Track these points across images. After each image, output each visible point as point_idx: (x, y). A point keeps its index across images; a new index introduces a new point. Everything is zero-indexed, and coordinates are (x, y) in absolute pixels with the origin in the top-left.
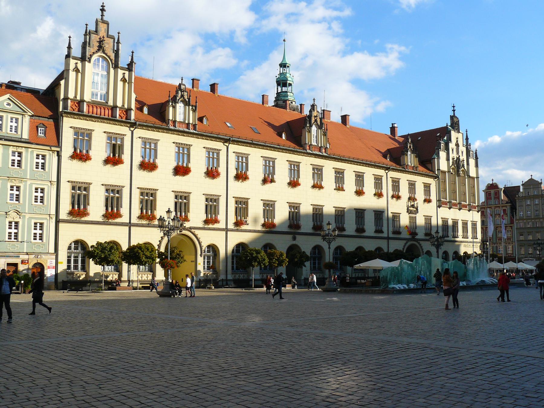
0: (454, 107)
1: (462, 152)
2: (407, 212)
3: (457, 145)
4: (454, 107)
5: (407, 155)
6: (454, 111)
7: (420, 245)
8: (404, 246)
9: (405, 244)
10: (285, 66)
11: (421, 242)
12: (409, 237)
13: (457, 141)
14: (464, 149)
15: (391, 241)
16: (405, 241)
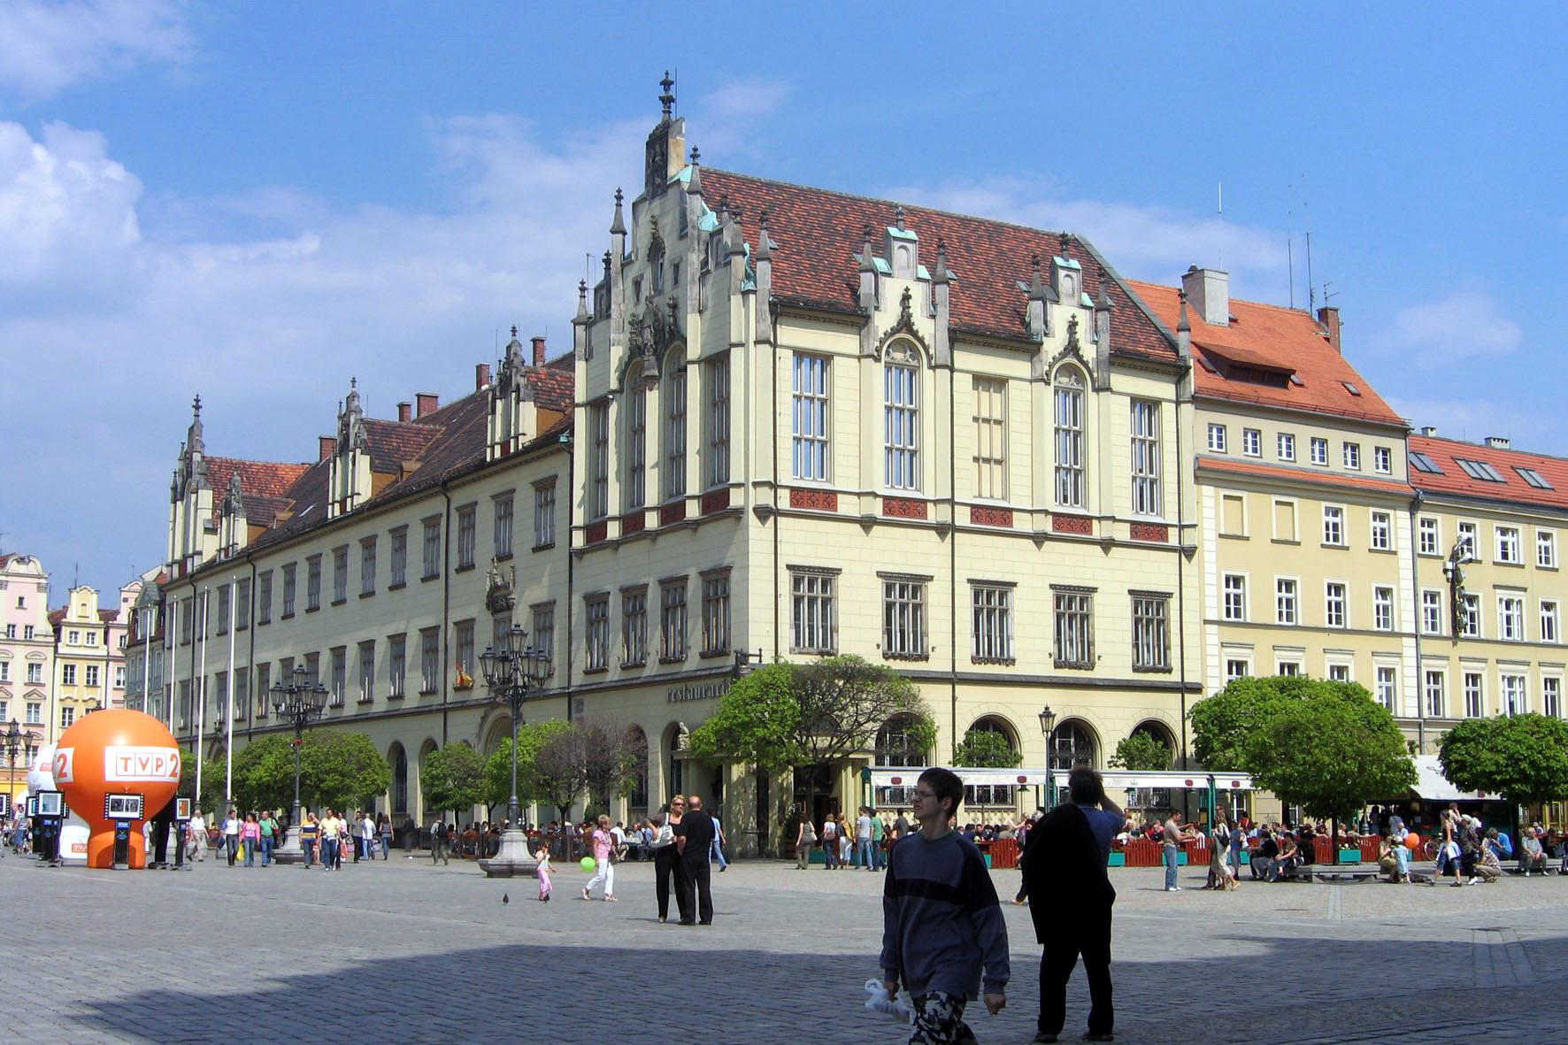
0: (667, 84)
4: (667, 84)
6: (667, 101)
15: (455, 719)
16: (480, 712)
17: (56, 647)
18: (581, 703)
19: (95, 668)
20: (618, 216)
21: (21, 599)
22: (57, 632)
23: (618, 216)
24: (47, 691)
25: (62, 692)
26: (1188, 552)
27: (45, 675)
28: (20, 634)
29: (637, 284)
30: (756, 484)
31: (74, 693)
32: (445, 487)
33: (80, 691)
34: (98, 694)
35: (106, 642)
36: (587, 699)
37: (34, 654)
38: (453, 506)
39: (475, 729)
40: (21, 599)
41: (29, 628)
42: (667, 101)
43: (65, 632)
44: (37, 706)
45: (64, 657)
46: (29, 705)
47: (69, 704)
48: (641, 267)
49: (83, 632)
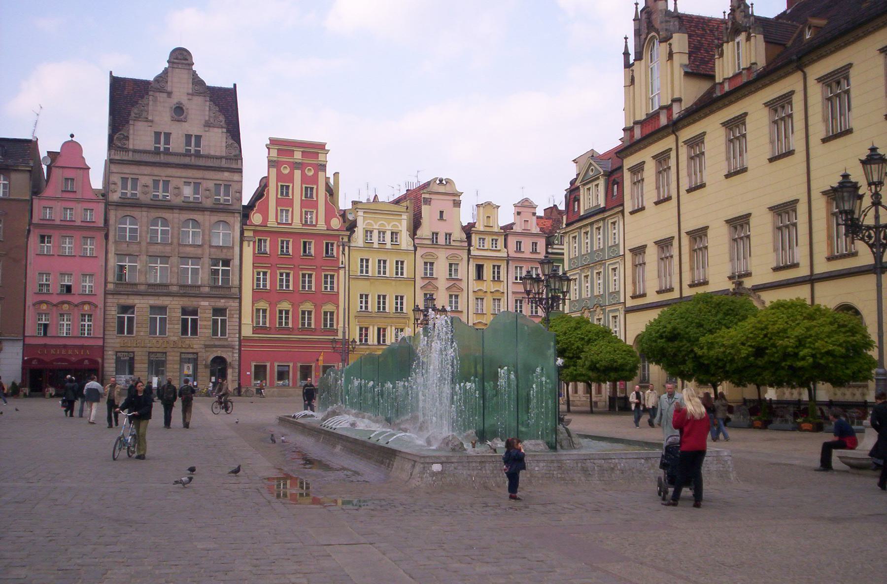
17: (469, 250)
19: (499, 267)
21: (441, 213)
22: (469, 237)
24: (464, 285)
25: (474, 285)
27: (462, 273)
28: (441, 240)
31: (483, 286)
33: (488, 285)
34: (502, 287)
35: (506, 247)
37: (454, 256)
40: (441, 213)
41: (448, 235)
43: (475, 239)
44: (457, 296)
45: (476, 257)
46: (451, 296)
47: (481, 295)
49: (488, 239)
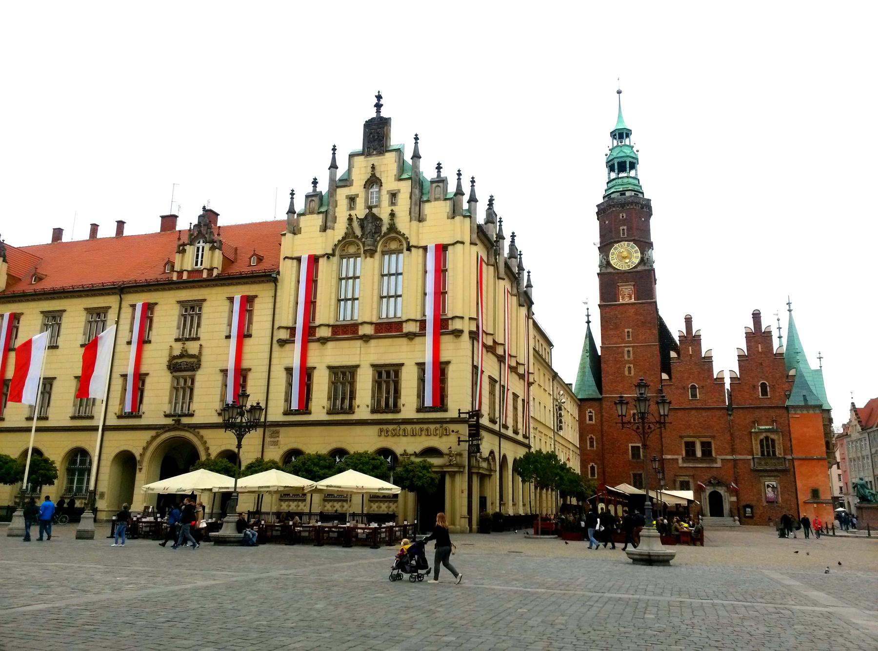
0: (379, 97)
1: (394, 195)
2: (169, 367)
3: (373, 181)
4: (379, 97)
5: (184, 251)
6: (378, 106)
7: (201, 438)
8: (149, 443)
9: (154, 438)
10: (621, 136)
11: (203, 432)
12: (169, 421)
13: (373, 175)
14: (405, 188)
16: (153, 433)
18: (278, 432)
20: (334, 159)
23: (334, 159)
26: (530, 384)
29: (352, 199)
30: (470, 319)
32: (121, 290)
36: (282, 430)
38: (125, 304)
39: (145, 445)
42: (378, 106)
48: (357, 188)
